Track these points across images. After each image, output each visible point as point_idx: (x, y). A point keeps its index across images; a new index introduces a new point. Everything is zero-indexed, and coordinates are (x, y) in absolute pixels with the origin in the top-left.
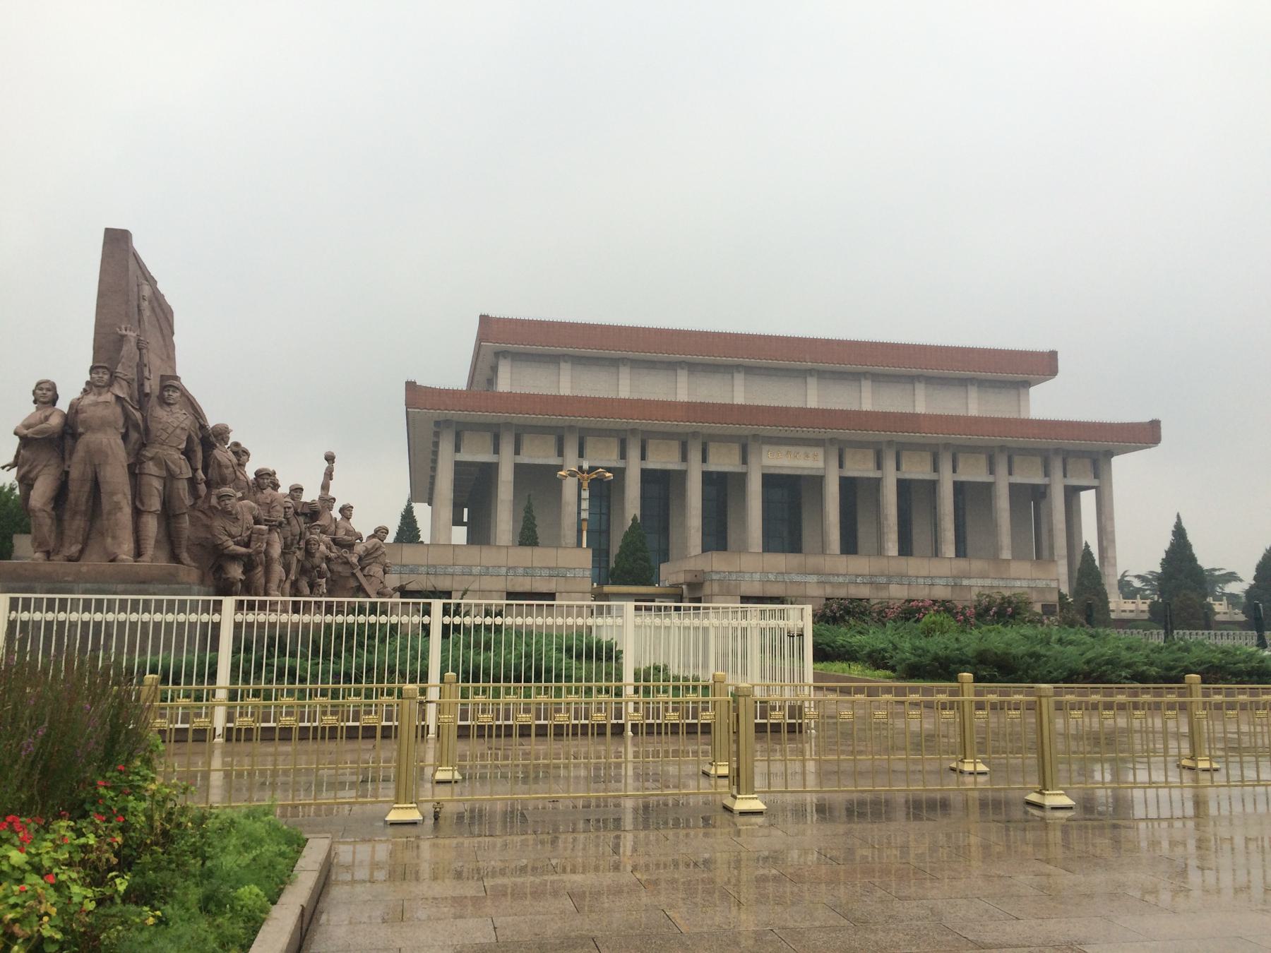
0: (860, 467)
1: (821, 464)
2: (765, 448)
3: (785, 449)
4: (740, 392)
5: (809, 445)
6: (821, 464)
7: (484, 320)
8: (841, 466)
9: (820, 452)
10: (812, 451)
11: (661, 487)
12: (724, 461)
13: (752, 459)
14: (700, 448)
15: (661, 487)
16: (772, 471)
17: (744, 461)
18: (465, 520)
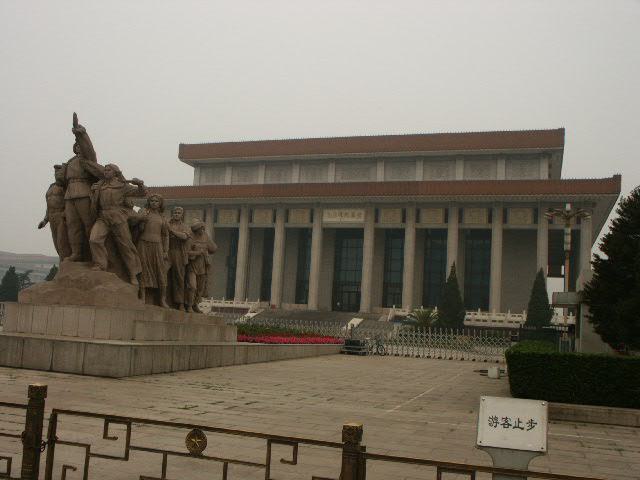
0: (389, 220)
1: (362, 220)
2: (326, 212)
3: (337, 211)
4: (331, 176)
5: (355, 207)
6: (362, 220)
7: (182, 147)
8: (376, 221)
9: (363, 212)
10: (357, 212)
11: (476, 242)
12: (299, 220)
13: (315, 220)
14: (373, 214)
15: (476, 242)
16: (329, 226)
17: (312, 221)
18: (563, 273)
